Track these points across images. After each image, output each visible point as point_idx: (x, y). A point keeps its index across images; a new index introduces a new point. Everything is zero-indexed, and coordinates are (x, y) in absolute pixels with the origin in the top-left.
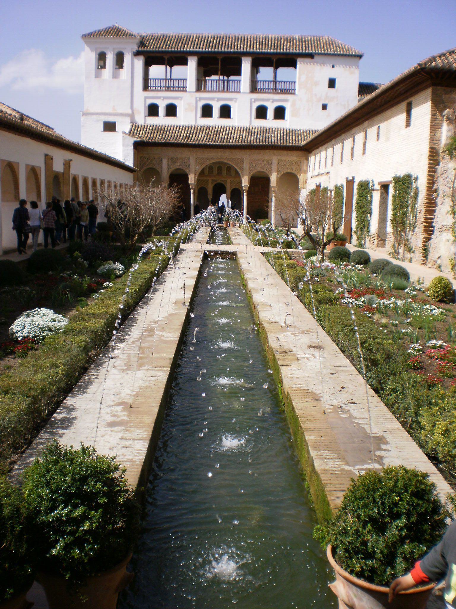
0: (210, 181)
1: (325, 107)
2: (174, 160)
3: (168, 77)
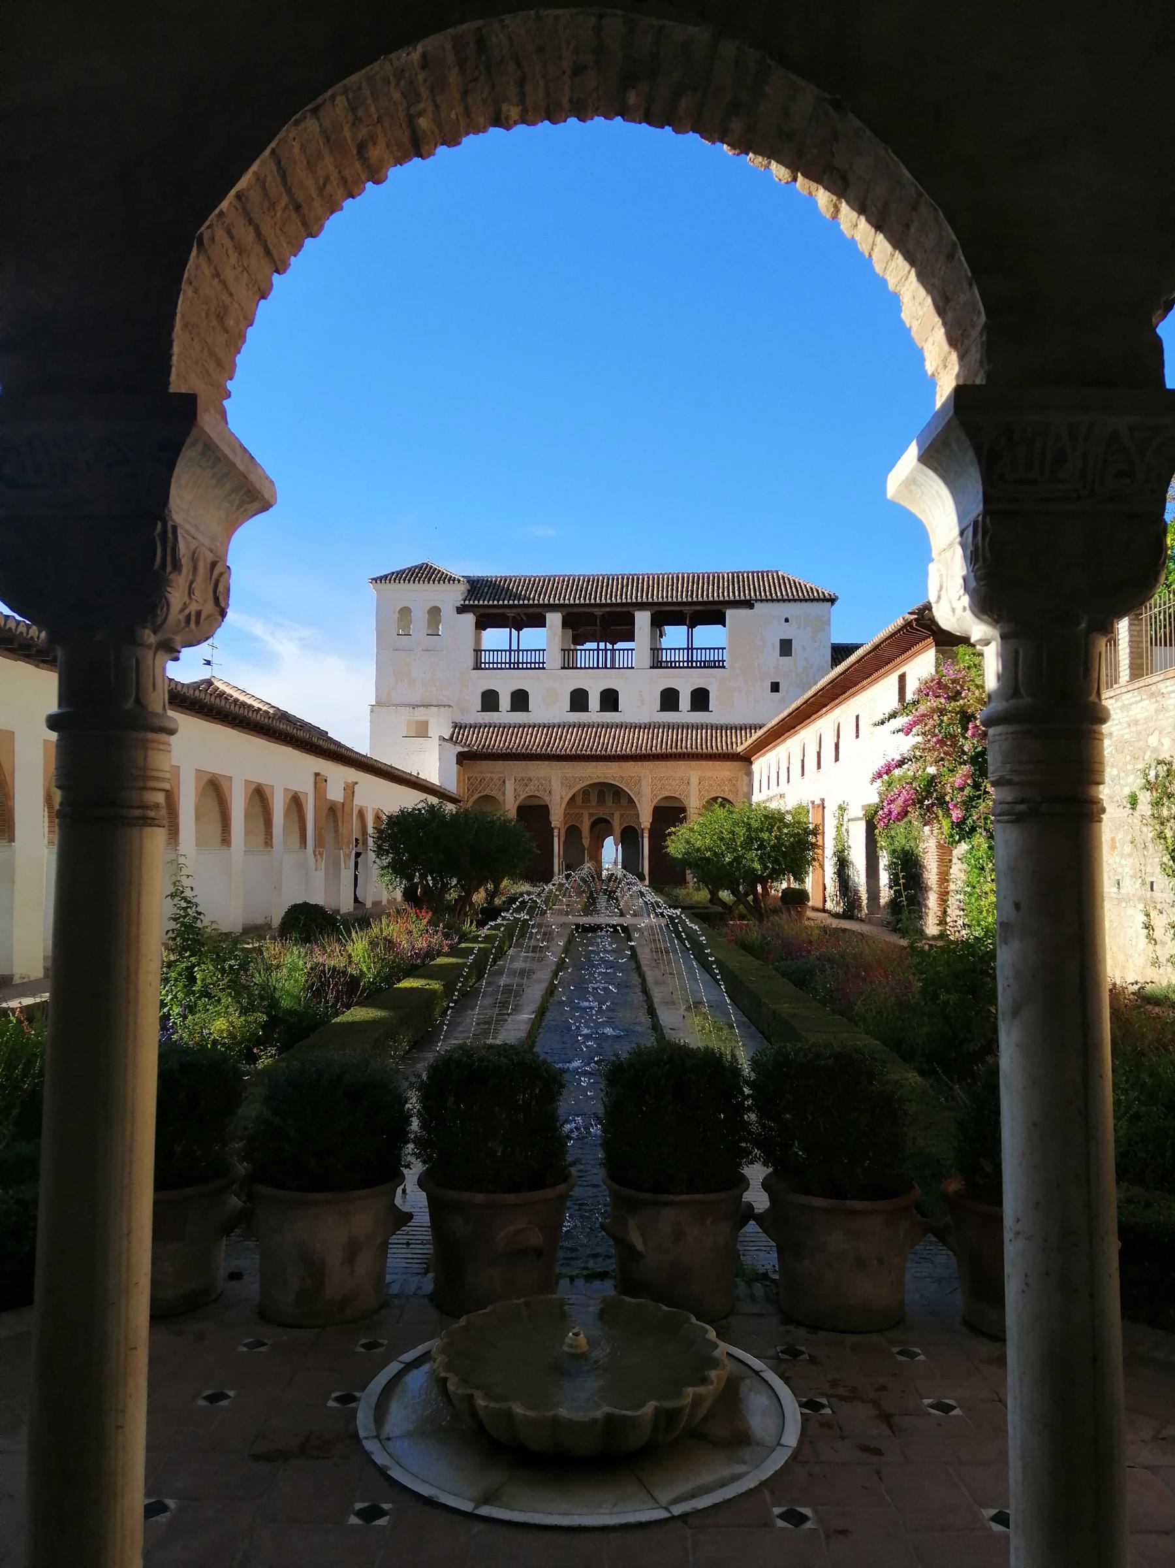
0: (586, 815)
1: (775, 687)
2: (525, 782)
3: (514, 647)
